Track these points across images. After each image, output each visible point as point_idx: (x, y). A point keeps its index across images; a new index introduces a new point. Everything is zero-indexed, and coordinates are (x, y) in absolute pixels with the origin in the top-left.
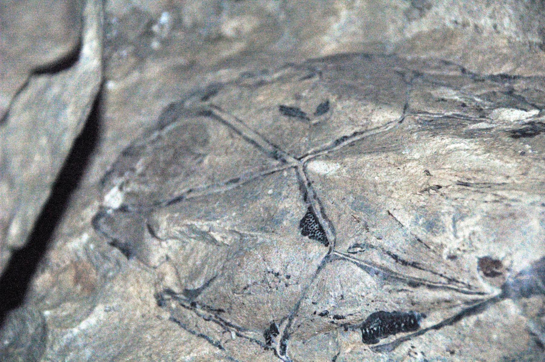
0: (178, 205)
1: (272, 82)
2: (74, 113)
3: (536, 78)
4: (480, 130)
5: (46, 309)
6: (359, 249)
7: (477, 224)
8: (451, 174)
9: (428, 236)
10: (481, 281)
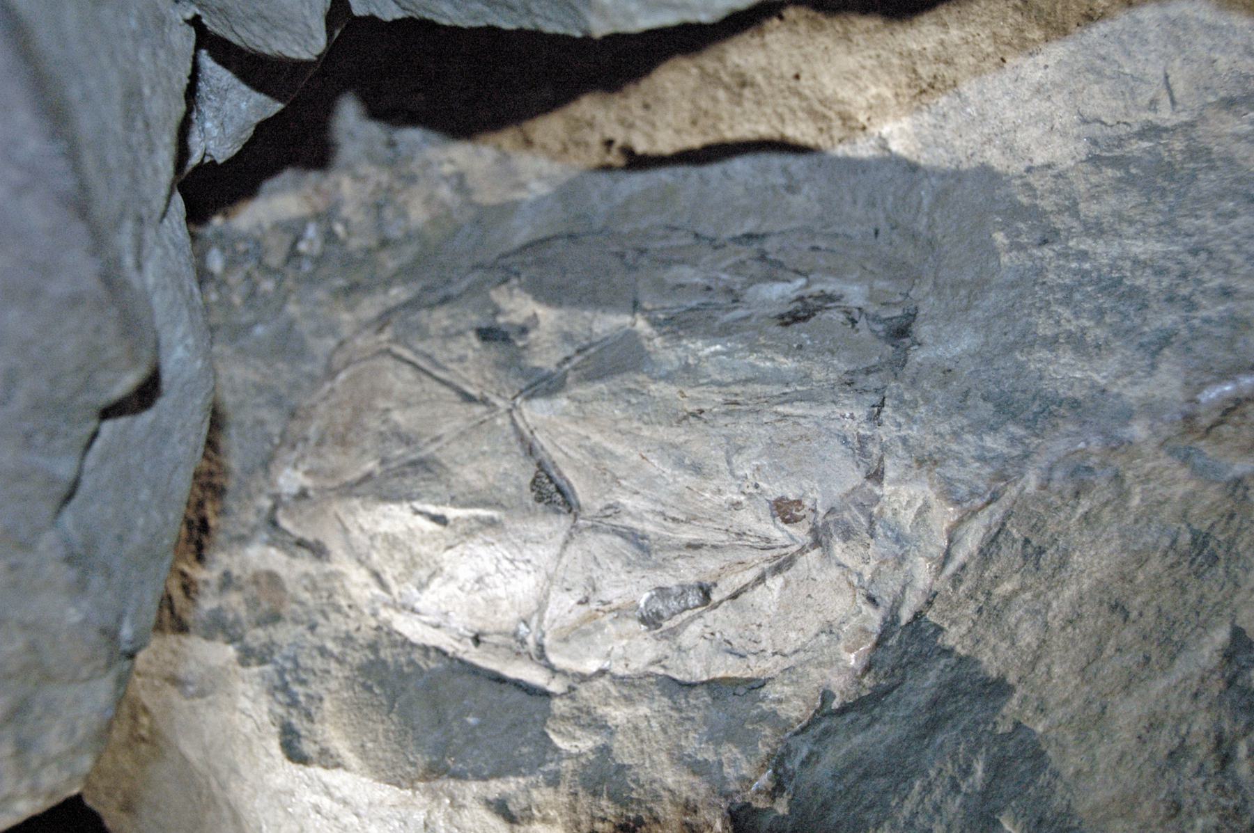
1: (460, 296)
4: (736, 320)
7: (760, 456)
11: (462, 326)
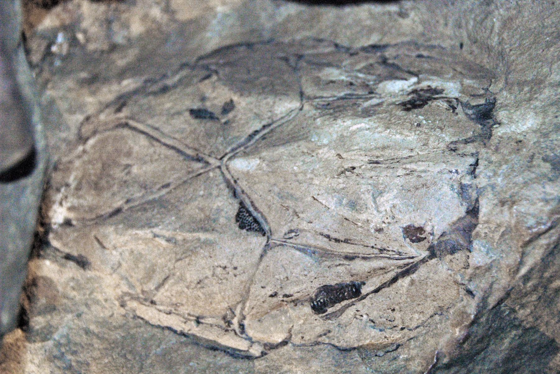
0: (119, 217)
1: (175, 86)
2: (33, 192)
3: (403, 43)
6: (293, 234)
7: (395, 197)
8: (361, 155)
9: (354, 214)
11: (178, 108)
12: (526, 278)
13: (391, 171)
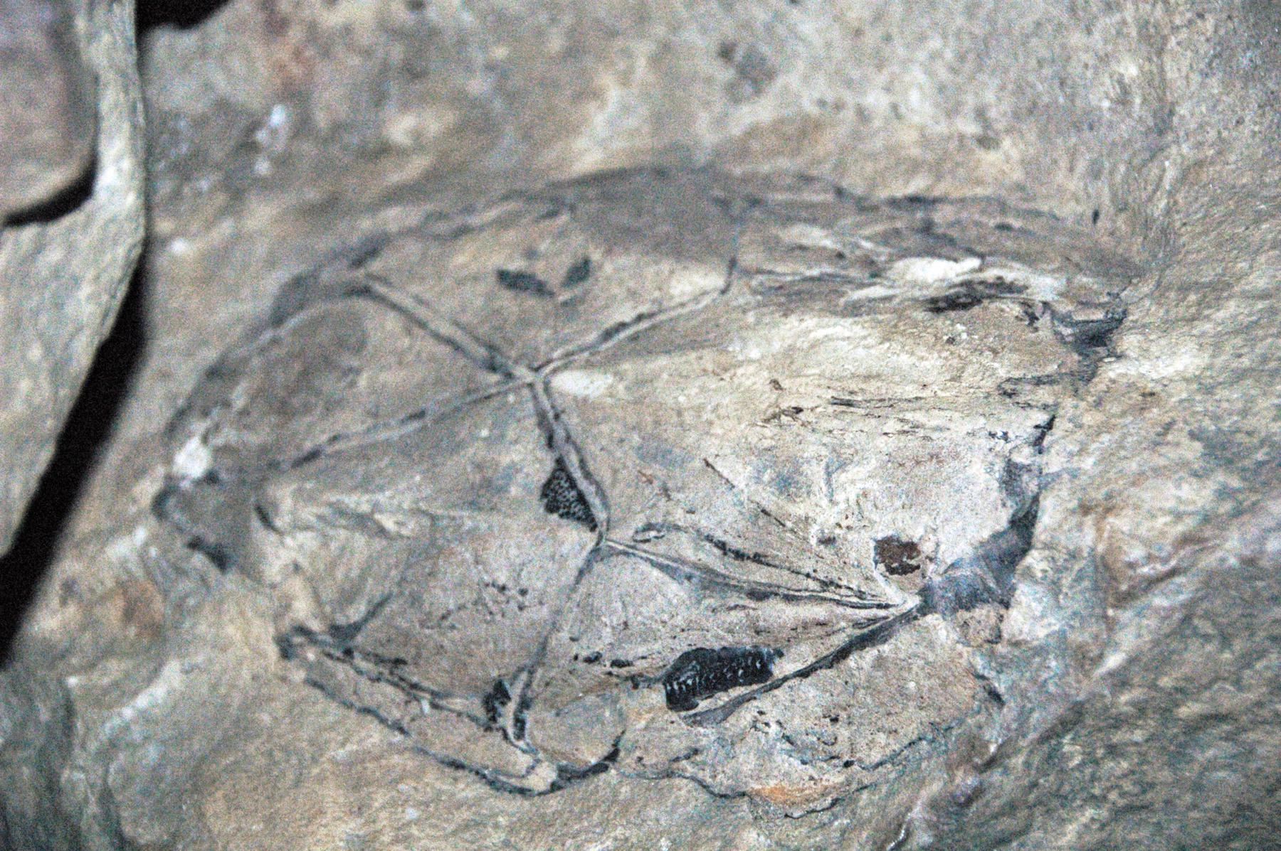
0: (311, 468)
1: (481, 228)
3: (975, 200)
4: (870, 300)
5: (71, 674)
6: (653, 534)
8: (819, 386)
9: (781, 503)
10: (881, 580)
12: (1120, 680)
13: (873, 421)
